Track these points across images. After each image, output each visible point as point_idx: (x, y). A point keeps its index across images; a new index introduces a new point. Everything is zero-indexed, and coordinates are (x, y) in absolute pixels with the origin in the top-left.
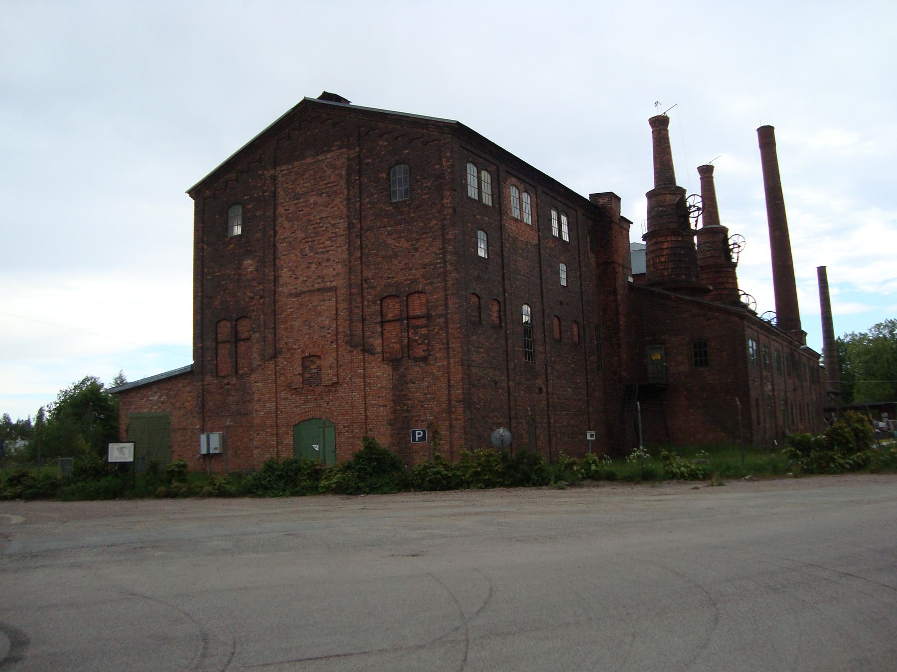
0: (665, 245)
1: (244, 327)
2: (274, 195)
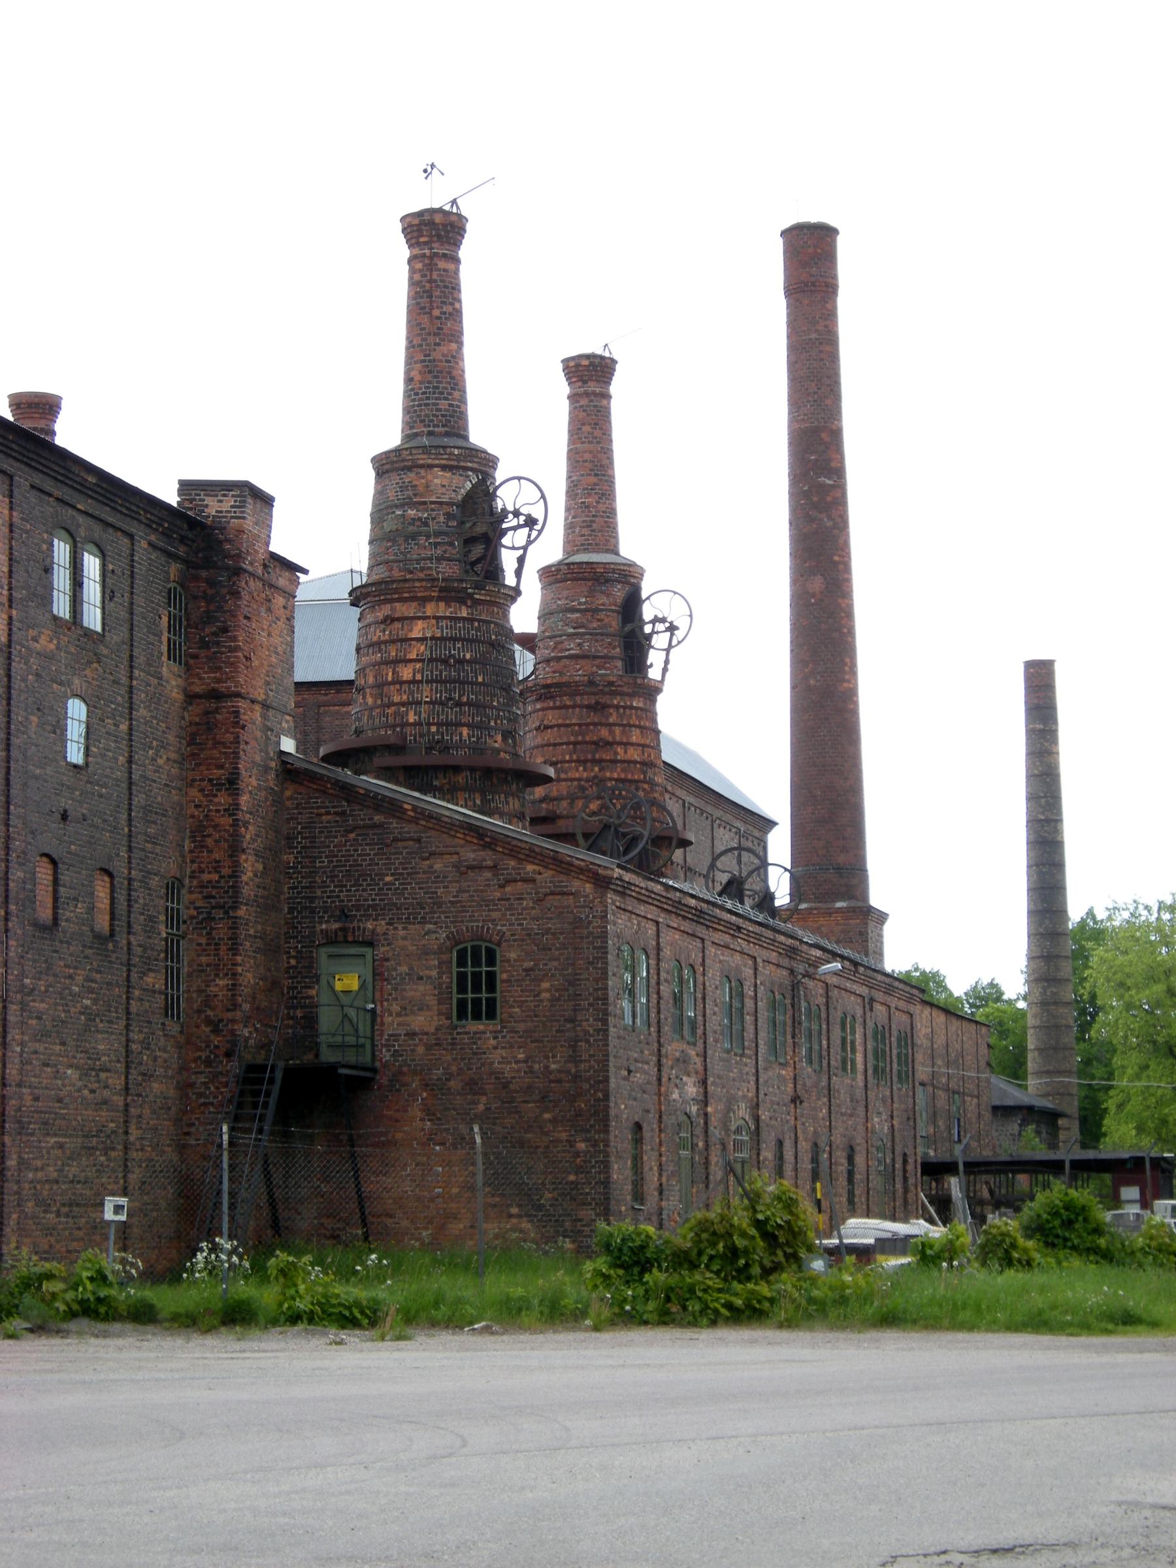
0: (417, 630)
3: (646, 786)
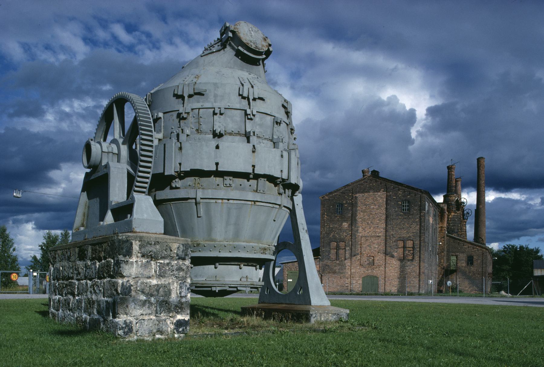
1: (342, 244)
2: (356, 203)
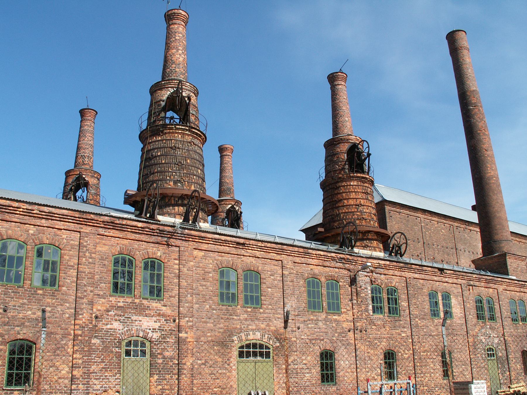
3: (359, 213)
